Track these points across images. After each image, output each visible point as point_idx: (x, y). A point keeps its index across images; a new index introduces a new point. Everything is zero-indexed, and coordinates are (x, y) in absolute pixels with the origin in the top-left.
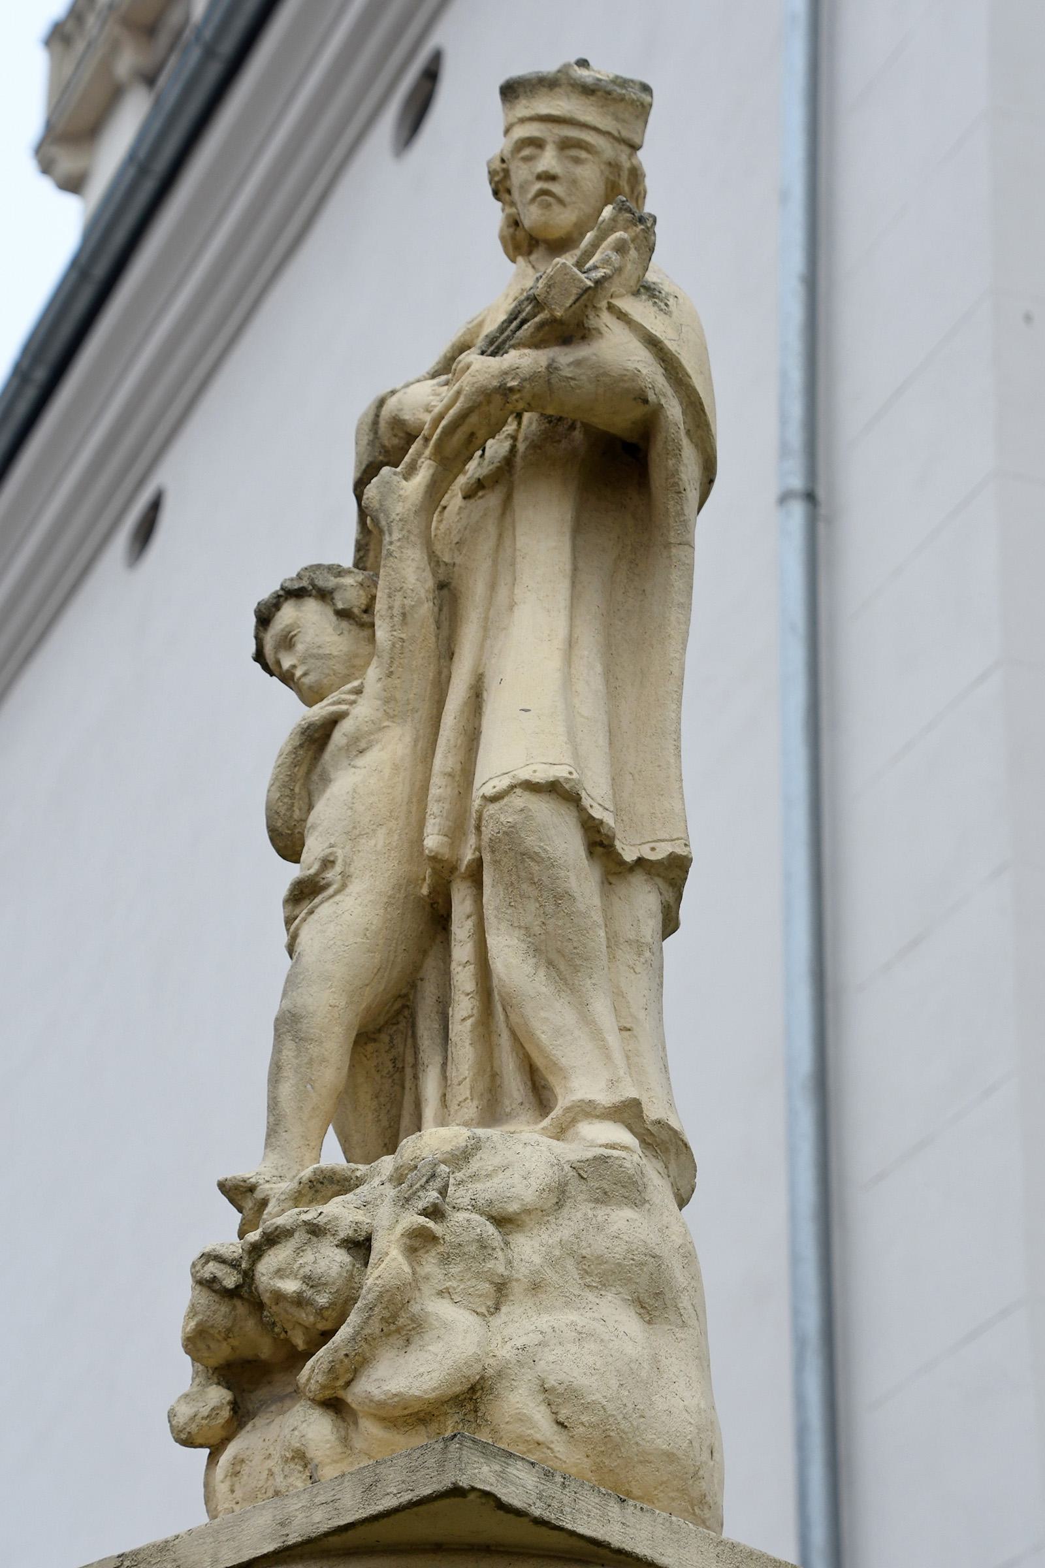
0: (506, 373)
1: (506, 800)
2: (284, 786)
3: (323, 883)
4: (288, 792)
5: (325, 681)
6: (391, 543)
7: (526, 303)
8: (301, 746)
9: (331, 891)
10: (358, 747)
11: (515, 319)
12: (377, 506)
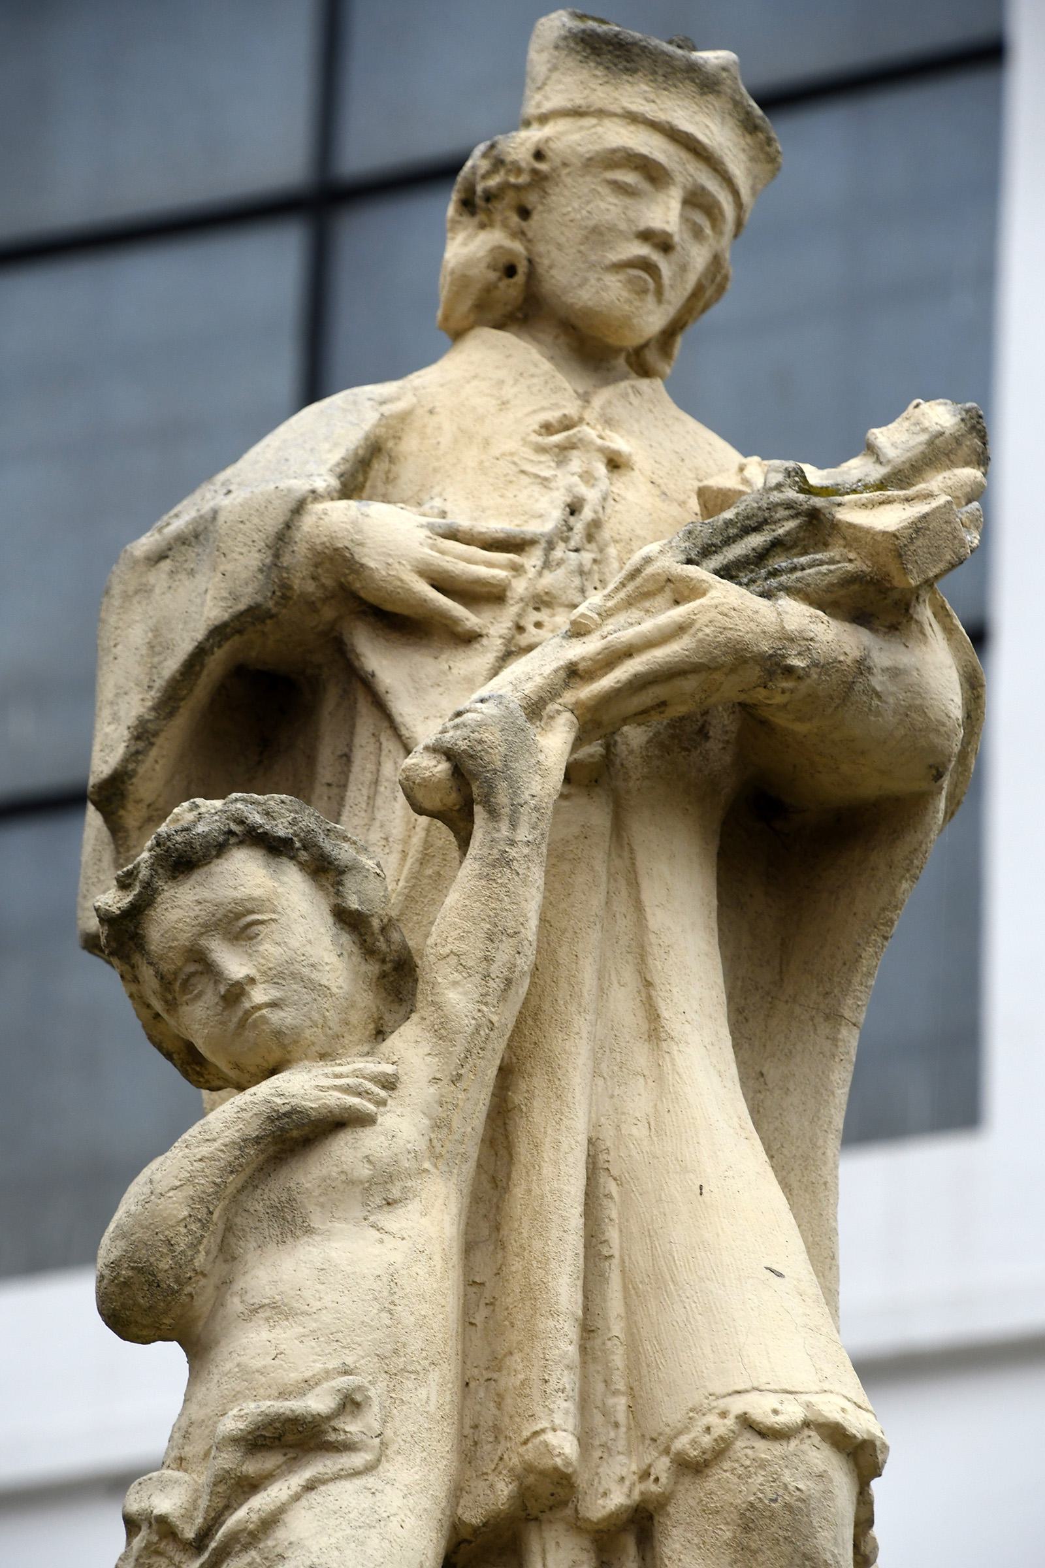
0: (792, 640)
1: (793, 1443)
2: (202, 1201)
3: (332, 1437)
4: (202, 1214)
5: (308, 1032)
6: (512, 843)
7: (781, 513)
8: (257, 1140)
9: (357, 1460)
10: (382, 1190)
11: (757, 529)
12: (499, 764)
